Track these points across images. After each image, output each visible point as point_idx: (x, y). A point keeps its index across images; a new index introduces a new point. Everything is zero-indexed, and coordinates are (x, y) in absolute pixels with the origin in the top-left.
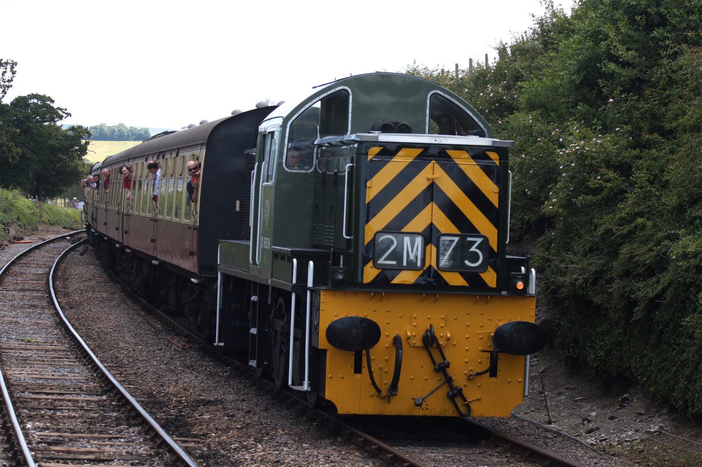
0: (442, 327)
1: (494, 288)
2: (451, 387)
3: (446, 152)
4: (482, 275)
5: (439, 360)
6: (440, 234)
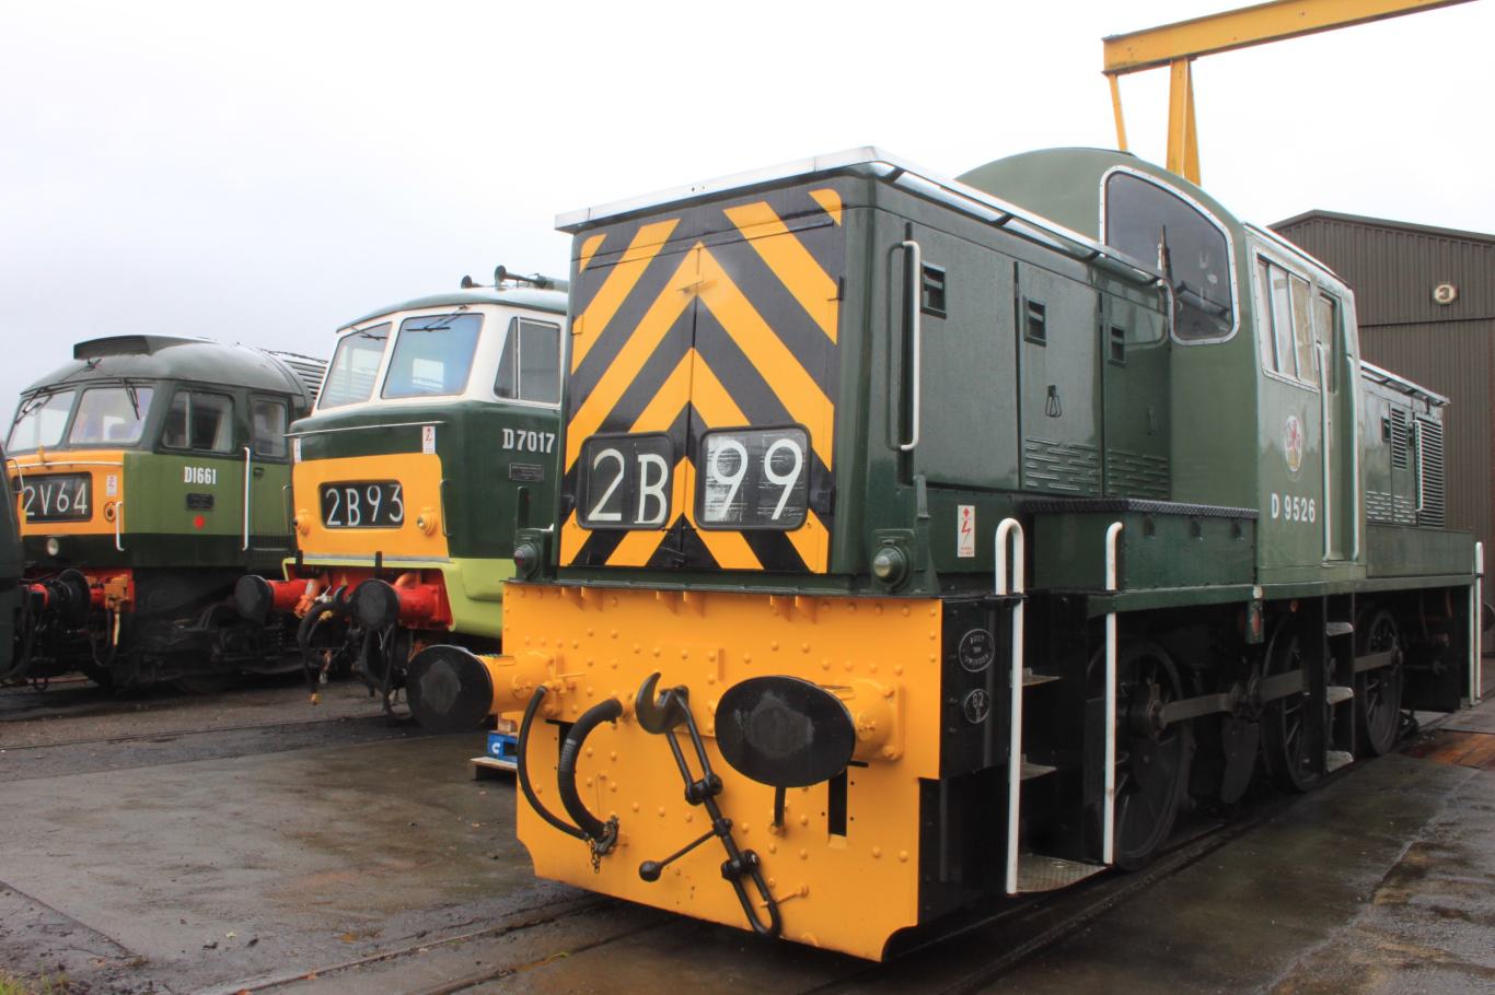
0: (712, 683)
1: (821, 575)
2: (731, 846)
3: (724, 214)
4: (788, 534)
5: (697, 774)
6: (705, 430)
